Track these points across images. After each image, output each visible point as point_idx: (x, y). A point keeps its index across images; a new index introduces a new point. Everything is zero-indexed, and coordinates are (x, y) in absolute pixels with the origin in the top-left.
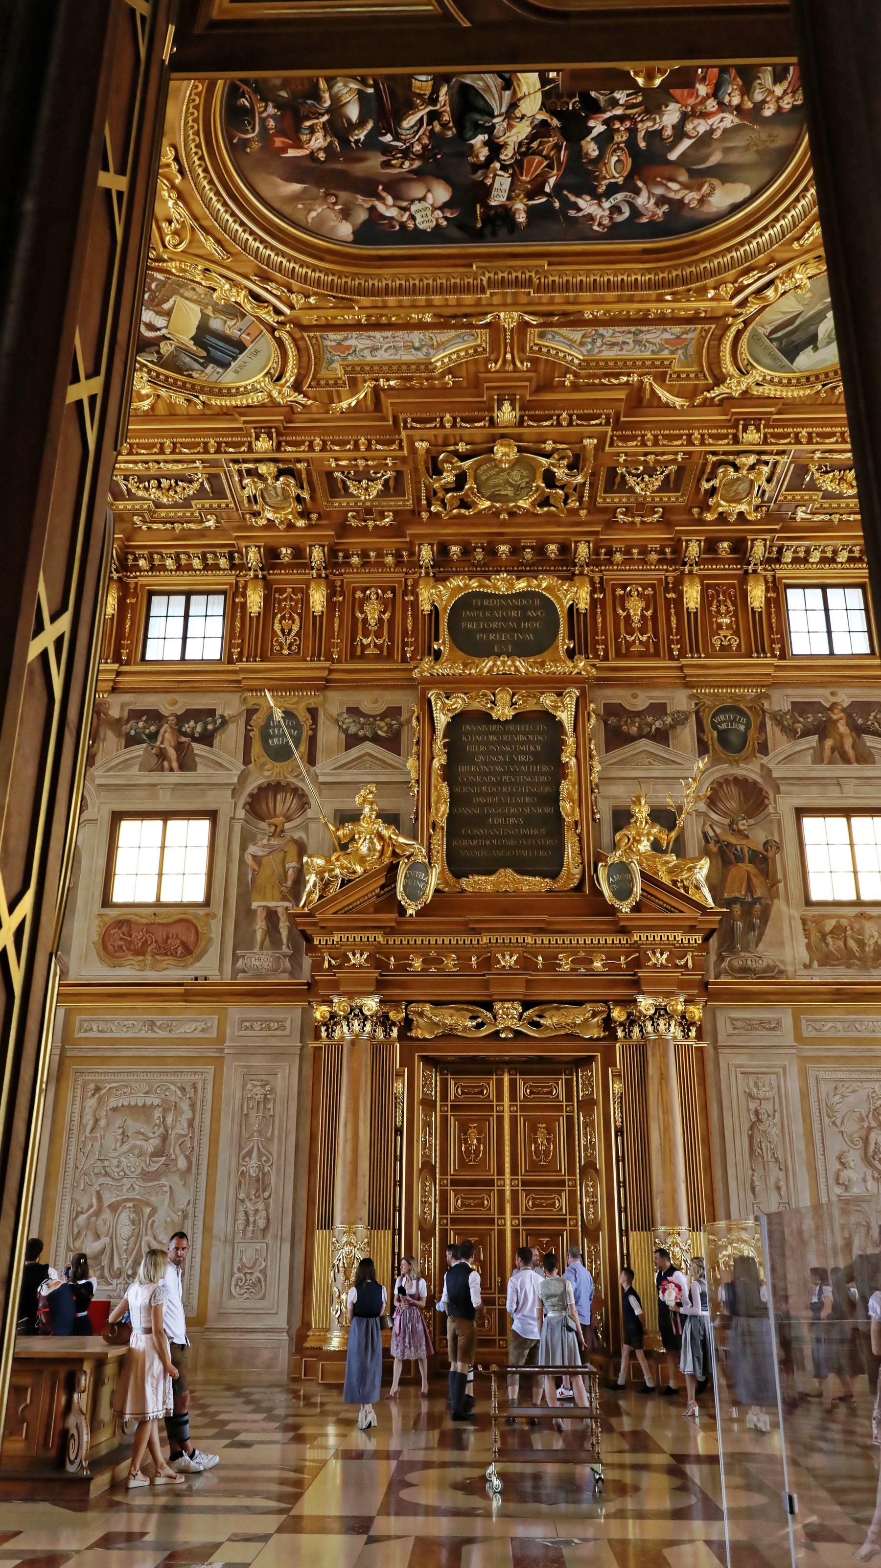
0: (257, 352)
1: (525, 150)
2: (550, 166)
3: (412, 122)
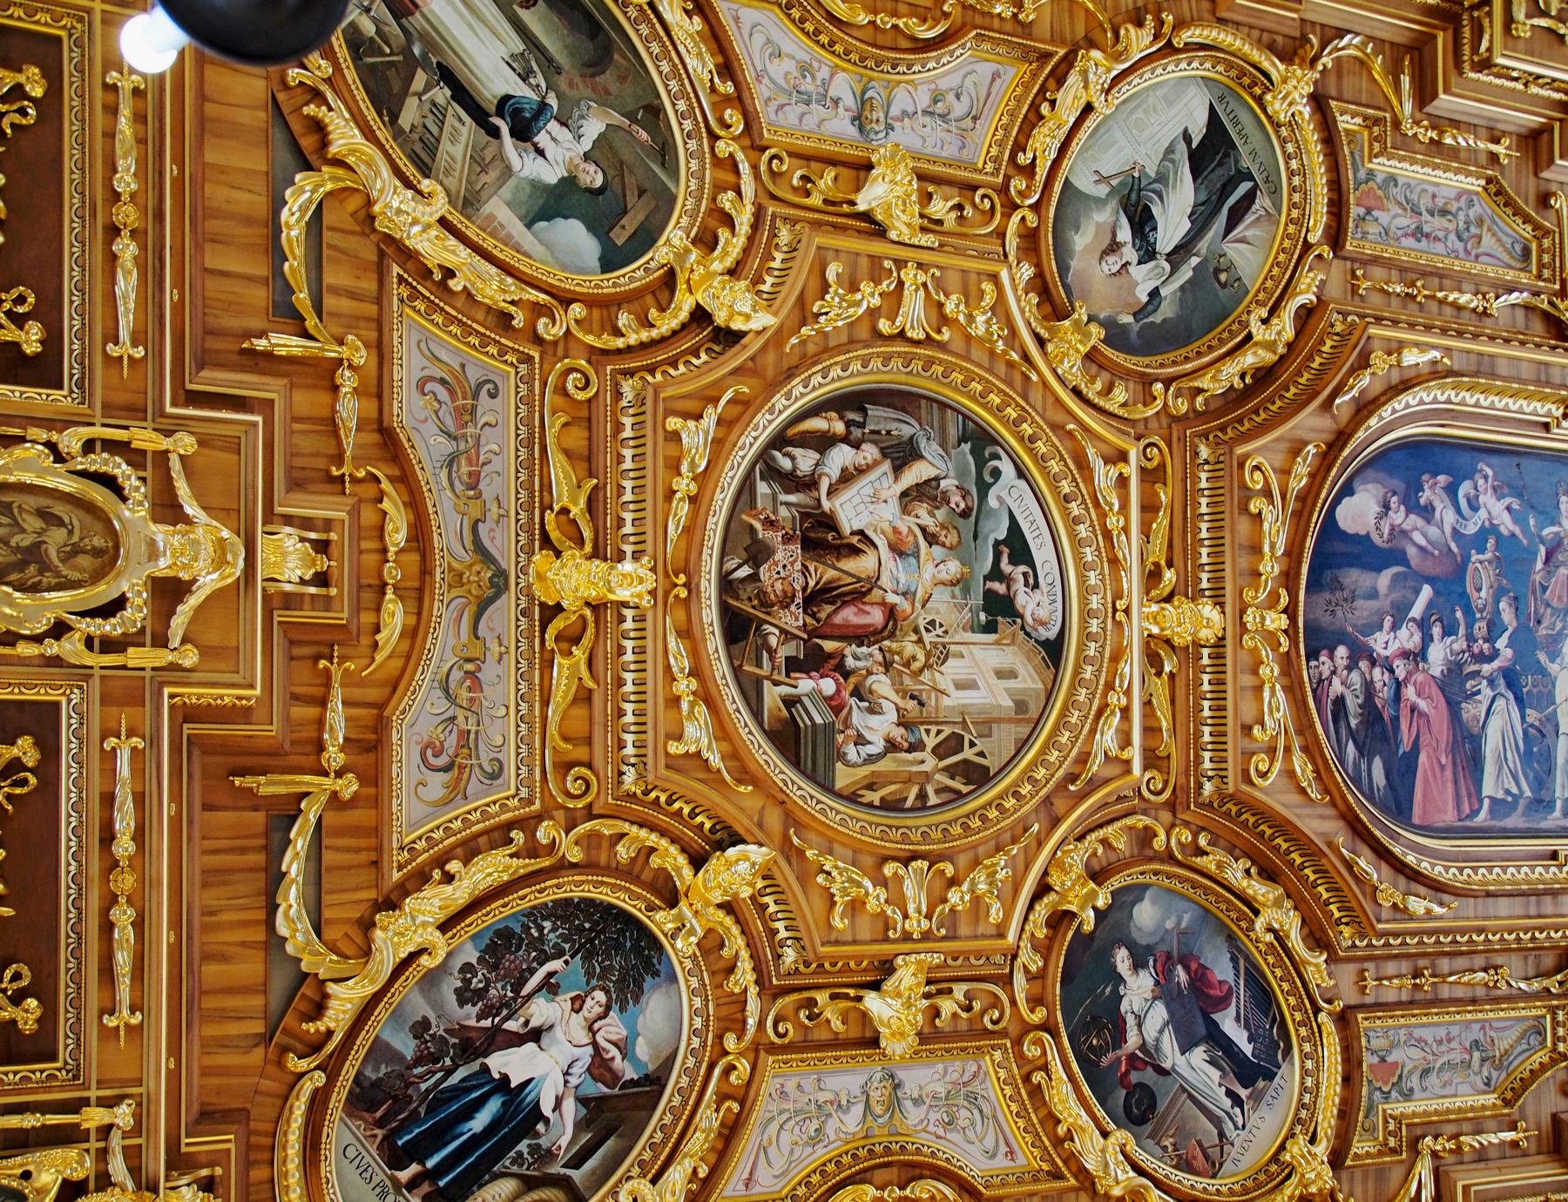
2: (1544, 589)
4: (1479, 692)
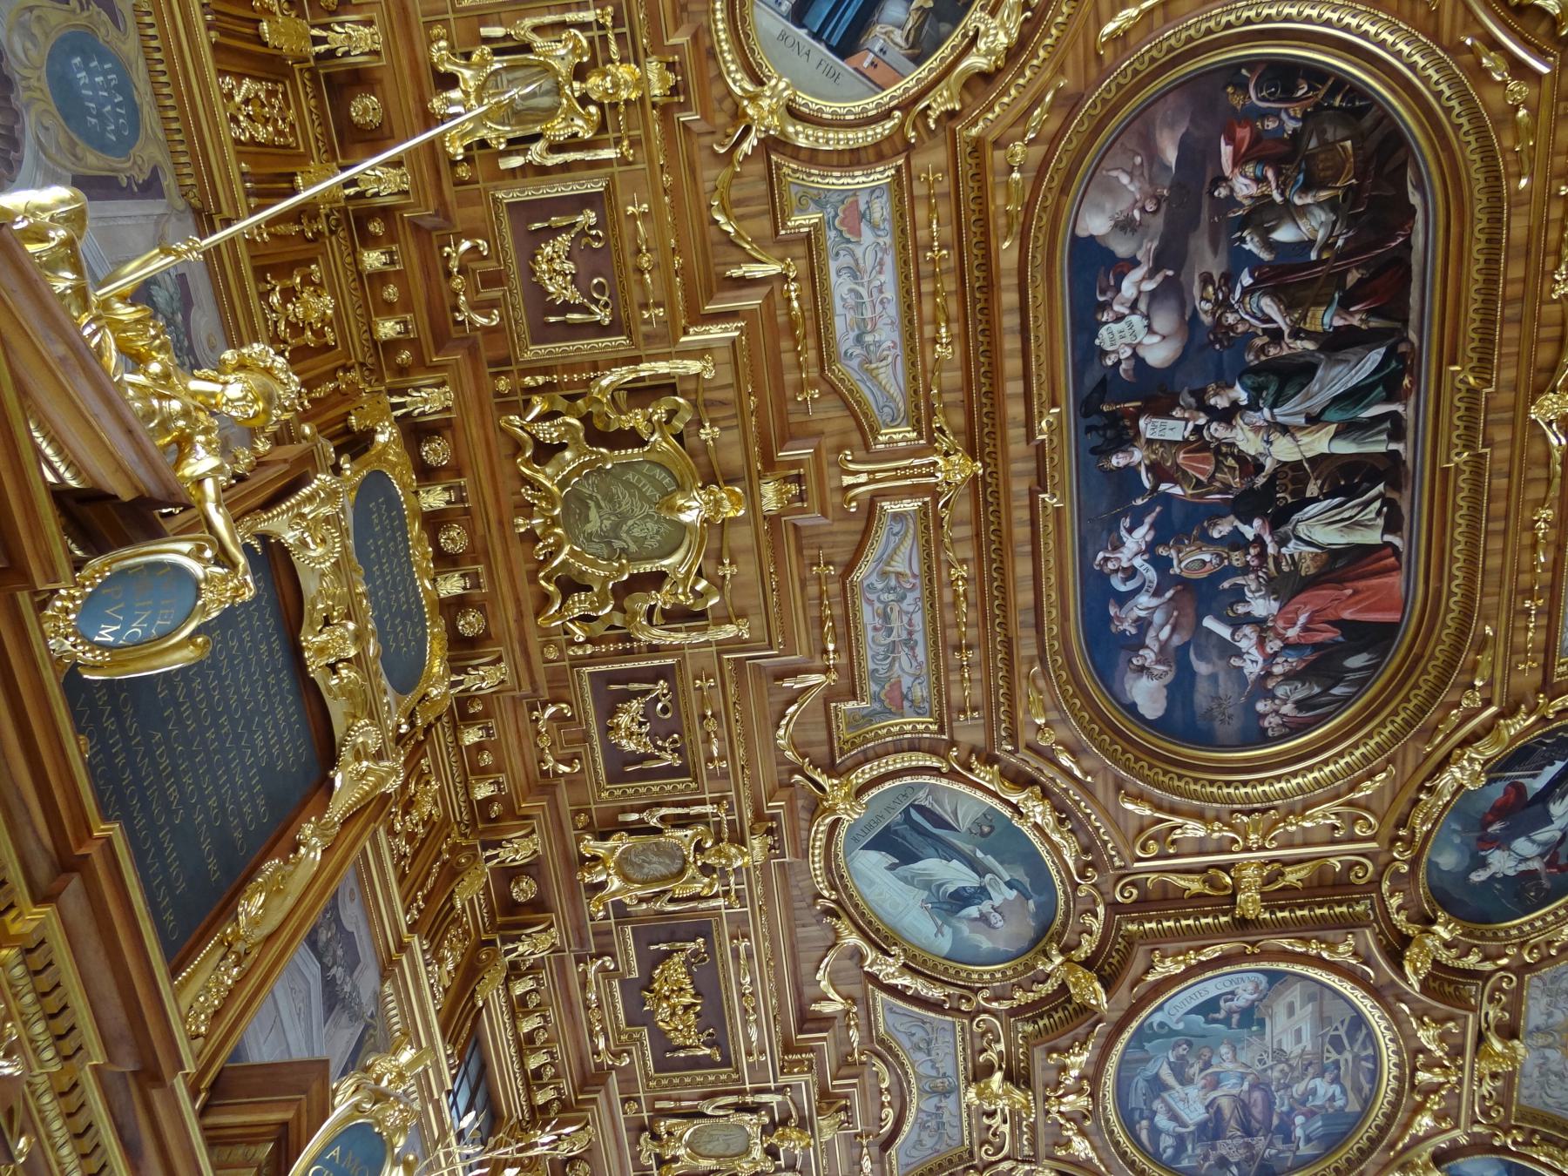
0: (836, 77)
1: (1221, 451)
2: (1199, 484)
3: (1267, 310)
4: (1292, 556)
